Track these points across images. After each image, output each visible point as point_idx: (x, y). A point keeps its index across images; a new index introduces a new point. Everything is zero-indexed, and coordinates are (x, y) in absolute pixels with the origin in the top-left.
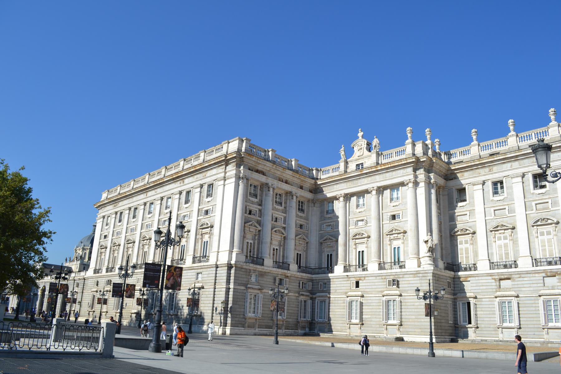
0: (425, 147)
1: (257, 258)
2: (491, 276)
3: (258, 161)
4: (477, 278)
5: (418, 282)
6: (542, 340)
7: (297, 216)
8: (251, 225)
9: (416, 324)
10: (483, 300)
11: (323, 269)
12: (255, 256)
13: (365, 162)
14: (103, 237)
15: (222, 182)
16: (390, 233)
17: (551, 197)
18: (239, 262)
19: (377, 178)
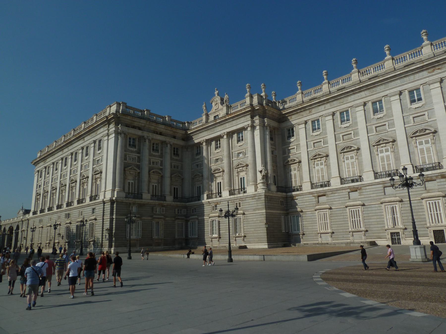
0: (260, 97)
1: (138, 194)
2: (312, 194)
3: (133, 119)
4: (302, 197)
5: (255, 203)
6: (349, 241)
7: (171, 159)
8: (131, 169)
9: (255, 235)
10: (307, 213)
11: (195, 198)
12: (136, 193)
13: (220, 114)
14: (38, 186)
15: (106, 138)
16: (238, 166)
17: (353, 129)
18: (119, 198)
19: (227, 125)
